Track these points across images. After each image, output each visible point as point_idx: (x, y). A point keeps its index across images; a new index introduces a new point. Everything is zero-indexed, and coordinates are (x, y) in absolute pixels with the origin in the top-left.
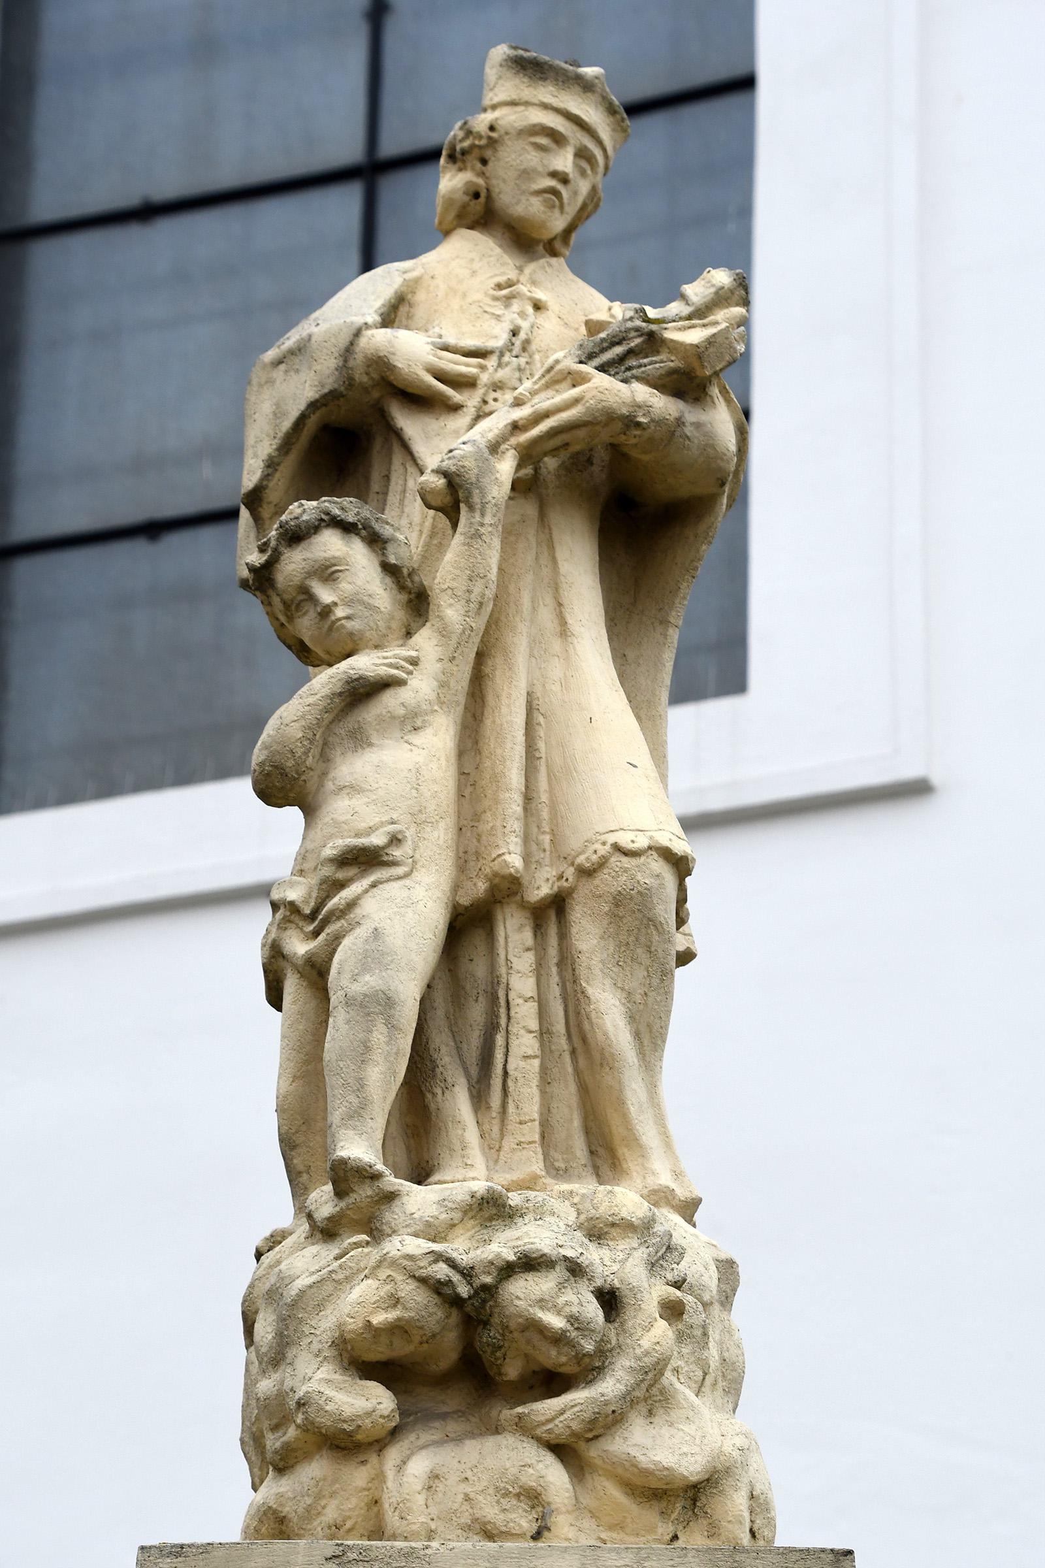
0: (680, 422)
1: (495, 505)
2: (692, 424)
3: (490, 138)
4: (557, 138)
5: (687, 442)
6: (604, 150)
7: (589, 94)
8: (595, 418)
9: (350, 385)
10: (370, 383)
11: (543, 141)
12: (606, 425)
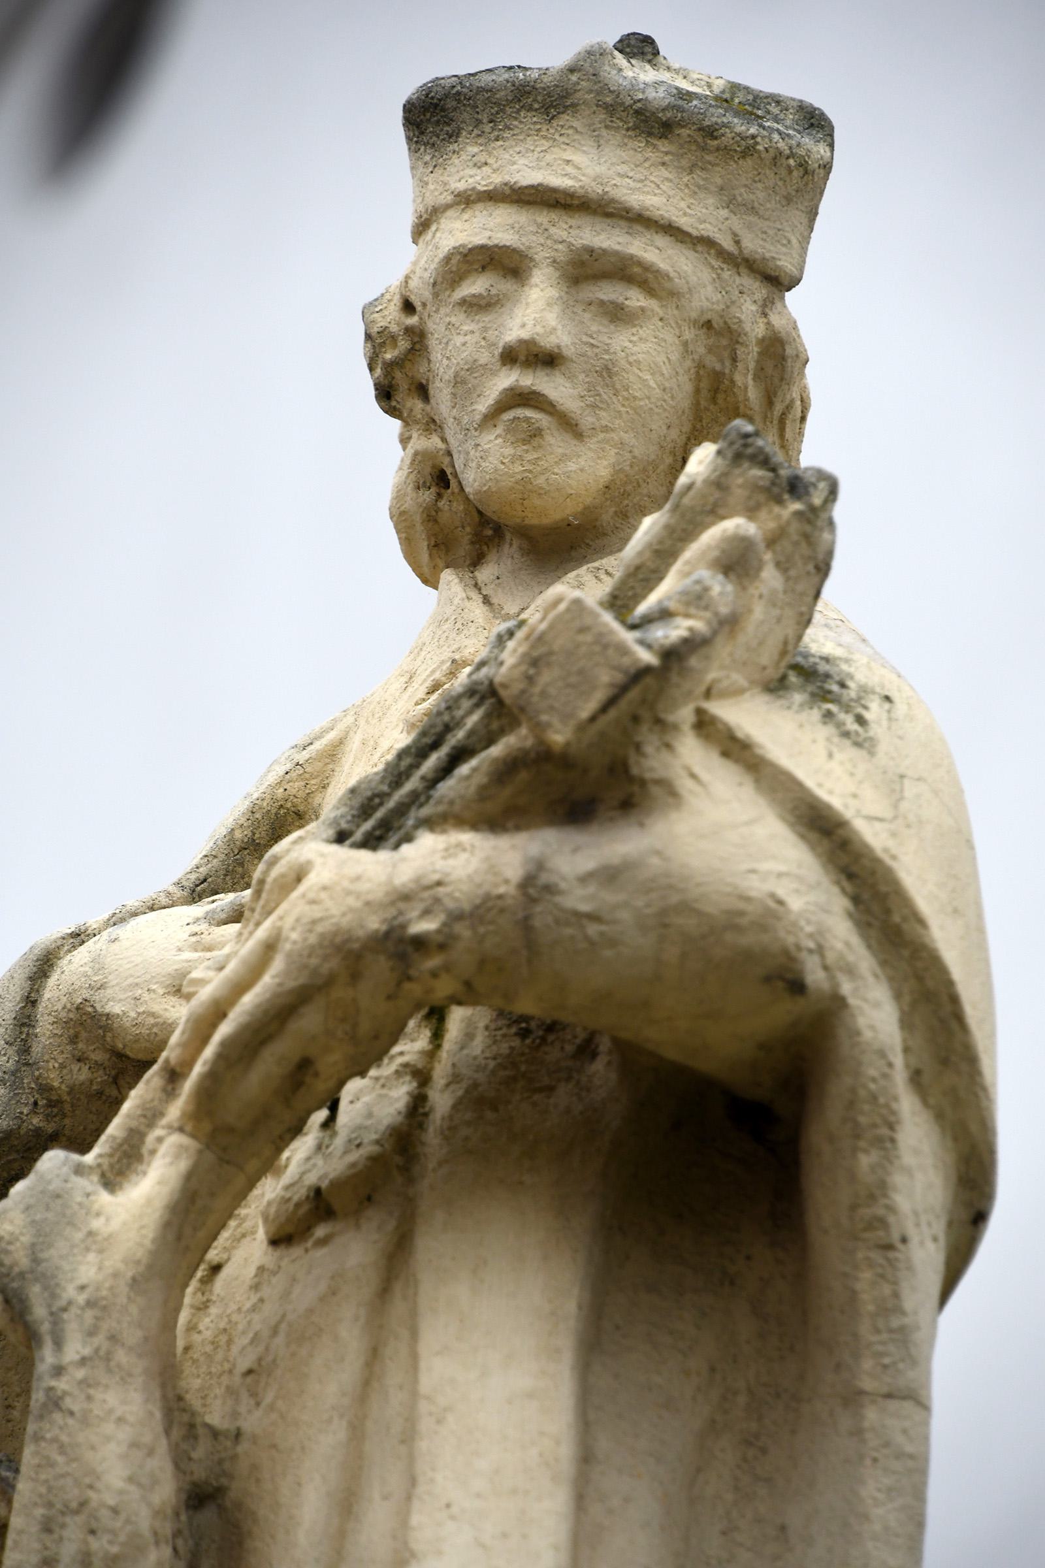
0: (536, 887)
1: (90, 1304)
2: (584, 879)
3: (409, 330)
4: (506, 264)
5: (593, 929)
6: (671, 230)
7: (564, 118)
8: (315, 972)
9: (51, 1104)
10: (100, 1076)
11: (476, 286)
12: (355, 977)
